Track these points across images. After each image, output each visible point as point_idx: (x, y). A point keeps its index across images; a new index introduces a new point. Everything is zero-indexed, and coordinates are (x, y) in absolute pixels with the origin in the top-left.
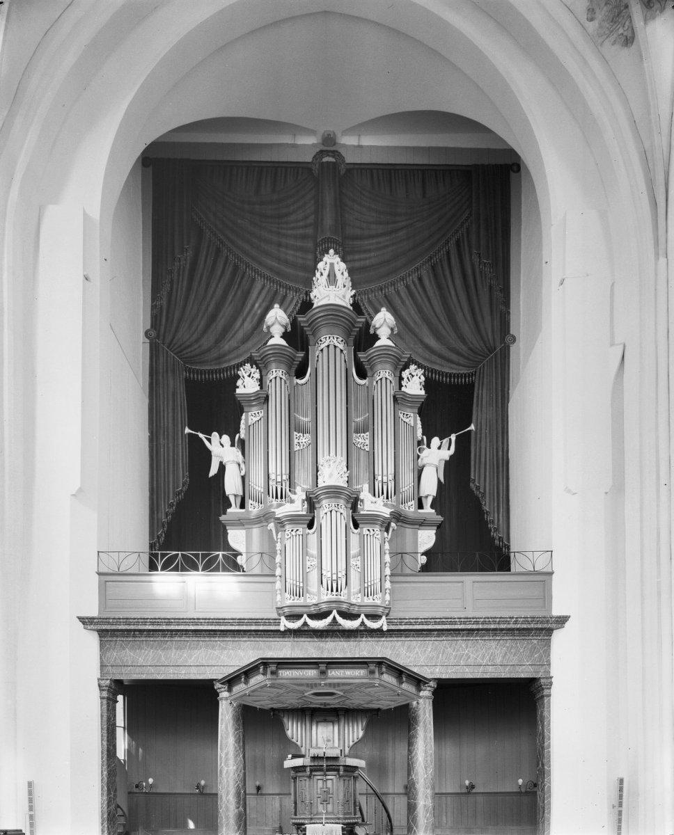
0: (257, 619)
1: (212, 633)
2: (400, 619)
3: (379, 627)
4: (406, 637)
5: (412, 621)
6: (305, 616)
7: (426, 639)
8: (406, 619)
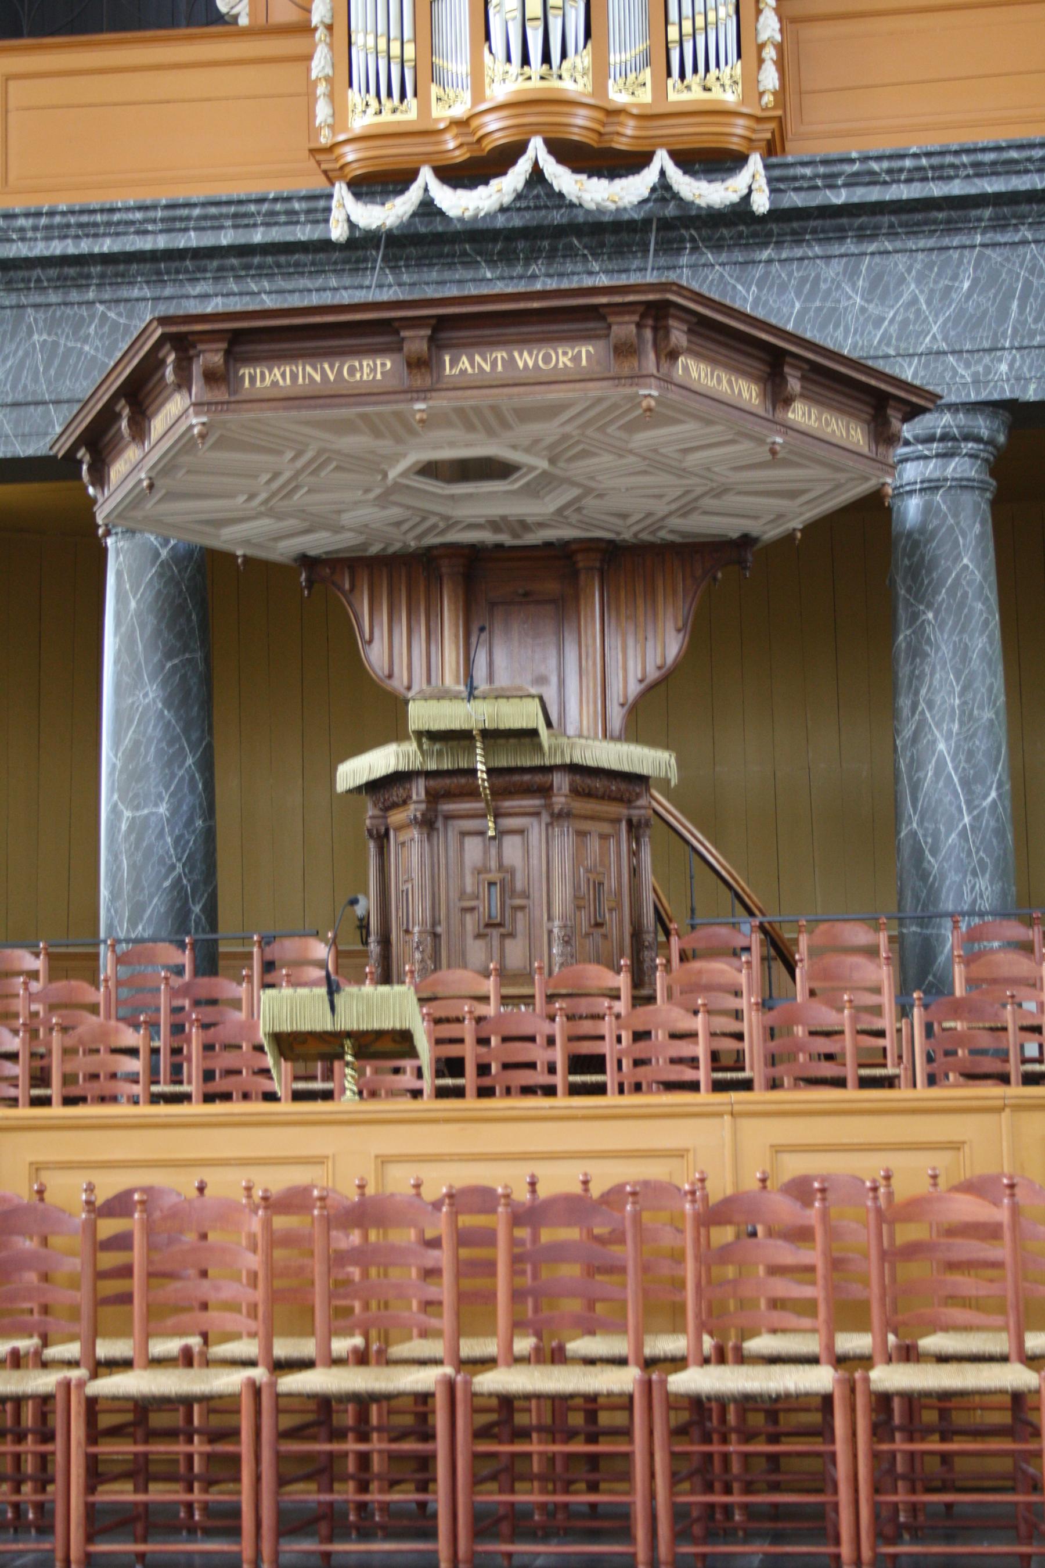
0: (240, 202)
1: (72, 271)
2: (825, 162)
3: (735, 198)
4: (861, 238)
5: (875, 166)
6: (426, 175)
7: (946, 241)
8: (852, 161)
